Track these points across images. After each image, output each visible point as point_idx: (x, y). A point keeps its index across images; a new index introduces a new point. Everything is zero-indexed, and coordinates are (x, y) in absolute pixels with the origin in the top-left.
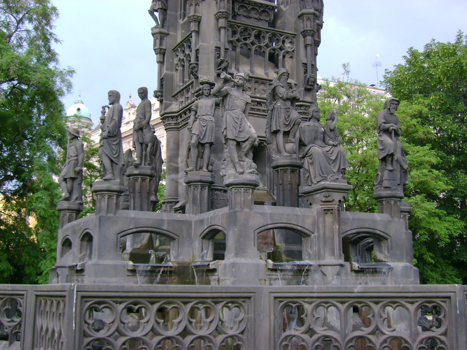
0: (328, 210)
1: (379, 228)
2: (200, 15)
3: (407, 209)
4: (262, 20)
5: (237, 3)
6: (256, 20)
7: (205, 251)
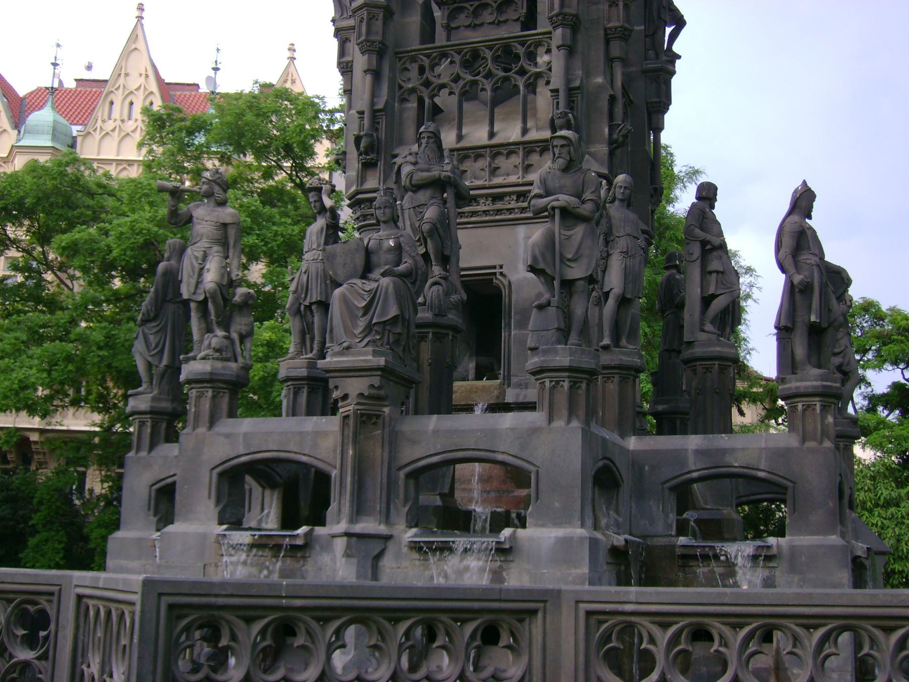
0: (370, 417)
1: (502, 449)
2: (350, 59)
3: (806, 387)
4: (506, 21)
5: (446, 7)
6: (492, 26)
7: (266, 512)
